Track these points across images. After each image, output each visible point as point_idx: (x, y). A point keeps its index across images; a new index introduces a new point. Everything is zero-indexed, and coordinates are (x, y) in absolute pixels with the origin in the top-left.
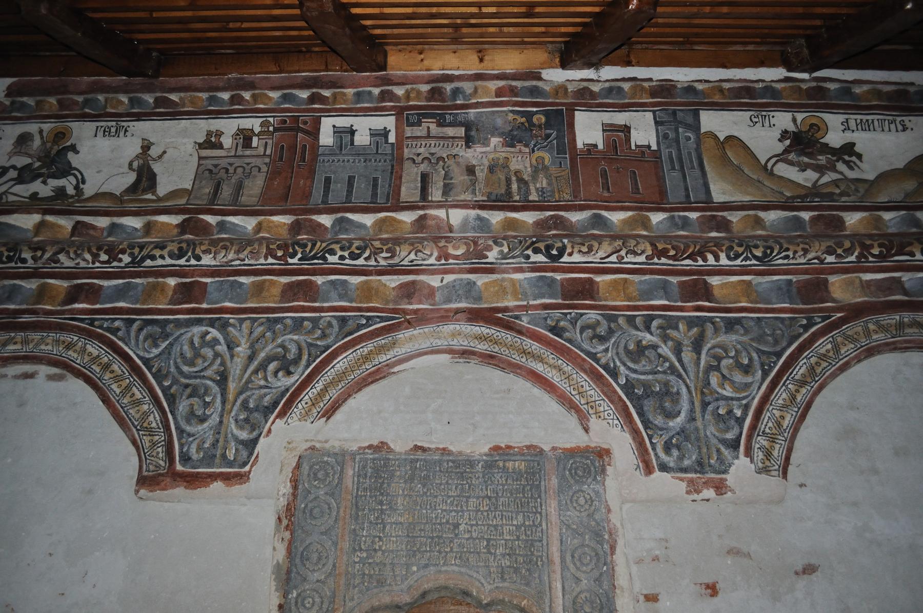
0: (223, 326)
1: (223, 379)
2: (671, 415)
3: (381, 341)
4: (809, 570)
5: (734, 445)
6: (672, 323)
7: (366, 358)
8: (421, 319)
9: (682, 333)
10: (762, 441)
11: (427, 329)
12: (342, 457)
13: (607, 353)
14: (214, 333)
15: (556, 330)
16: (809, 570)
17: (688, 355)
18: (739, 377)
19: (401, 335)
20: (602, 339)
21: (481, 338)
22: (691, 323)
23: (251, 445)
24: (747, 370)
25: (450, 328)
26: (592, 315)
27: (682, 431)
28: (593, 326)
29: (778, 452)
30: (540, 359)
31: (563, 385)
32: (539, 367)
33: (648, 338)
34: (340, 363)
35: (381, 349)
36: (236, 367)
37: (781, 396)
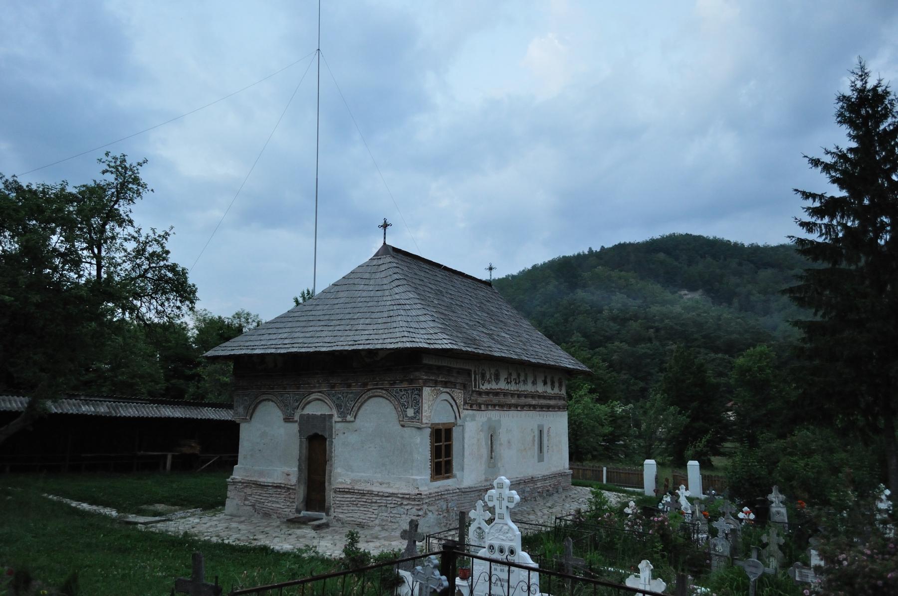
0: (289, 394)
1: (290, 404)
2: (341, 409)
3: (308, 397)
4: (356, 431)
5: (348, 414)
6: (343, 393)
7: (306, 400)
8: (313, 393)
9: (345, 395)
10: (352, 412)
11: (314, 394)
12: (305, 415)
13: (334, 398)
14: (288, 396)
15: (329, 395)
16: (356, 431)
17: (345, 399)
18: (350, 403)
19: (311, 395)
20: (334, 396)
21: (321, 396)
22: (346, 392)
23: (294, 414)
24: (352, 401)
25: (316, 394)
26: (334, 392)
27: (342, 412)
28: (333, 394)
29: (354, 414)
30: (327, 399)
31: (329, 404)
32: (326, 401)
33: (340, 396)
34: (303, 401)
35: (308, 398)
36: (291, 401)
37: (356, 405)
